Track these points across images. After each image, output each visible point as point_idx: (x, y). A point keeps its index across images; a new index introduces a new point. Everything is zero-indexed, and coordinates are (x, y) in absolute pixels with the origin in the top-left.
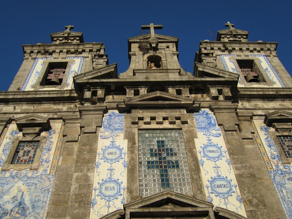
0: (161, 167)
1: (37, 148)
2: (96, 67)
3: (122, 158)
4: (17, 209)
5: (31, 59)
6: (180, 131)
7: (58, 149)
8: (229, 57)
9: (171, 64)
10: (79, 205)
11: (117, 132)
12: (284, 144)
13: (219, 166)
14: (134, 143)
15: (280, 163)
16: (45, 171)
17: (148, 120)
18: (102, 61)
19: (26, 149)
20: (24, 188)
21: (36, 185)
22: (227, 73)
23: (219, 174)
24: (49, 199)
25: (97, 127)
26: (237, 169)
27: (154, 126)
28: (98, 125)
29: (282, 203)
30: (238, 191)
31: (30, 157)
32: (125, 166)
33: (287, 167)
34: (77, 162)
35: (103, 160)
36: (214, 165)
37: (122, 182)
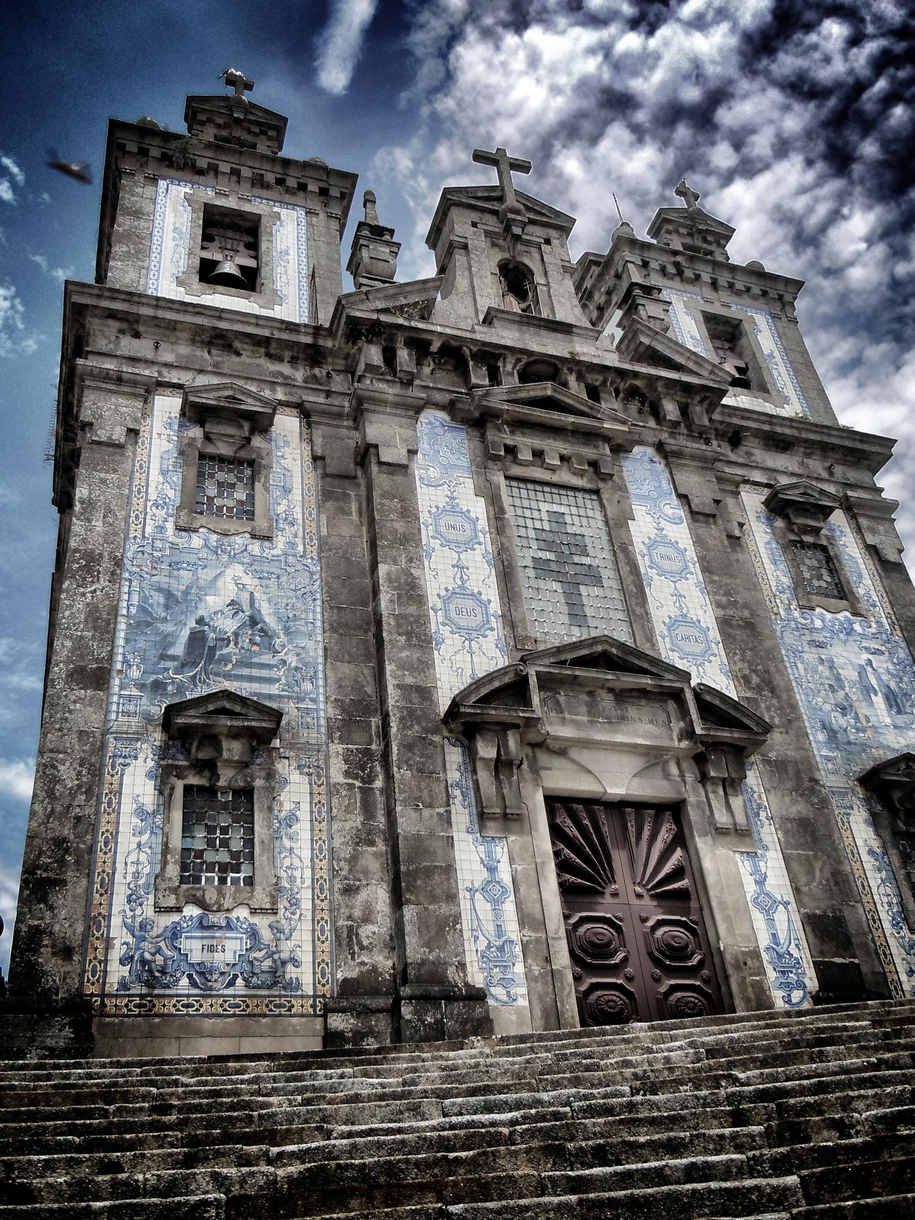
7: (309, 491)
10: (408, 640)
14: (502, 511)
19: (221, 476)
20: (247, 580)
21: (278, 577)
22: (706, 365)
23: (685, 611)
24: (319, 616)
25: (409, 451)
26: (719, 605)
28: (410, 447)
30: (723, 654)
33: (806, 616)
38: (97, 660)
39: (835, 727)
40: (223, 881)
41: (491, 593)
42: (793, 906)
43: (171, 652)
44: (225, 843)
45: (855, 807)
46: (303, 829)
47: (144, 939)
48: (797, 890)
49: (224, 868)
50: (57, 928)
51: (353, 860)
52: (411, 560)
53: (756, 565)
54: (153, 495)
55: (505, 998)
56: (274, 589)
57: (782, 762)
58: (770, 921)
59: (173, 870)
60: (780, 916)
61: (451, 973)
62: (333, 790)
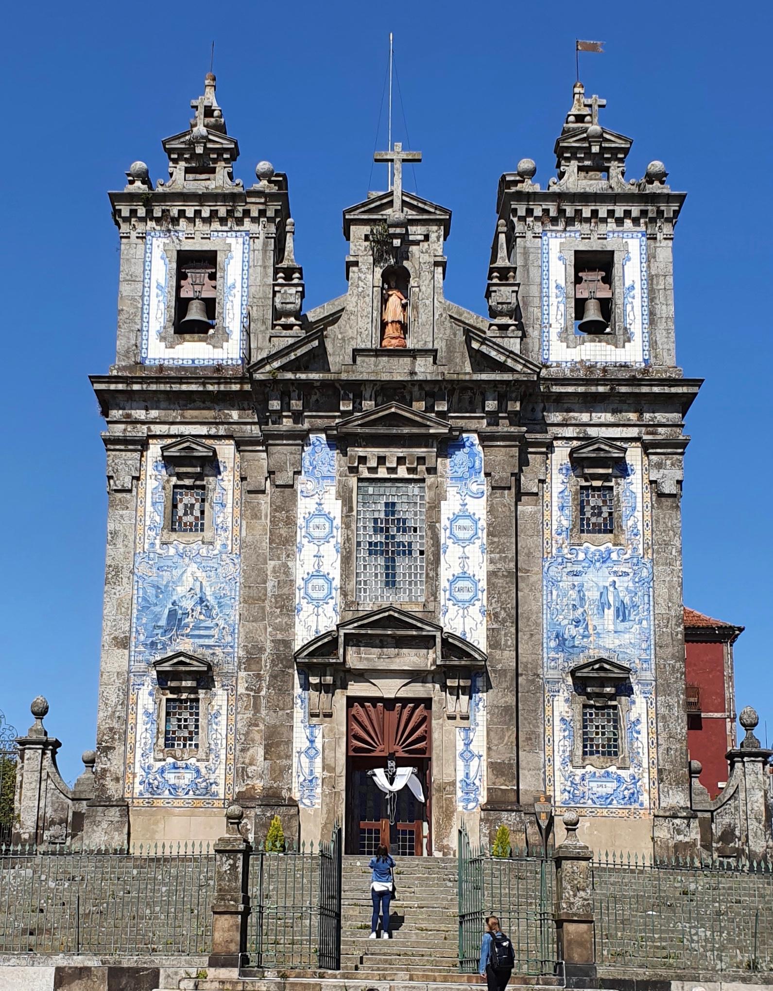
0: (387, 552)
1: (203, 500)
2: (282, 308)
3: (333, 537)
4: (199, 608)
5: (137, 237)
6: (422, 485)
8: (563, 240)
9: (427, 302)
10: (281, 611)
11: (326, 482)
12: (588, 503)
13: (468, 555)
14: (351, 509)
15: (567, 542)
16: (225, 546)
17: (373, 463)
18: (293, 290)
19: (188, 499)
20: (199, 574)
24: (238, 593)
25: (295, 473)
26: (492, 561)
27: (382, 473)
29: (545, 612)
31: (196, 518)
32: (337, 551)
34: (271, 541)
35: (307, 539)
36: (460, 554)
37: (333, 579)
38: (124, 633)
39: (566, 637)
40: (185, 746)
41: (336, 574)
42: (485, 757)
43: (159, 624)
44: (186, 727)
45: (561, 691)
46: (223, 719)
47: (148, 773)
48: (489, 749)
49: (185, 739)
50: (112, 769)
51: (247, 734)
52: (288, 556)
53: (545, 513)
54: (148, 523)
55: (309, 804)
56: (213, 580)
57: (505, 670)
58: (467, 766)
59: (162, 741)
60: (475, 763)
61: (284, 793)
62: (239, 698)
